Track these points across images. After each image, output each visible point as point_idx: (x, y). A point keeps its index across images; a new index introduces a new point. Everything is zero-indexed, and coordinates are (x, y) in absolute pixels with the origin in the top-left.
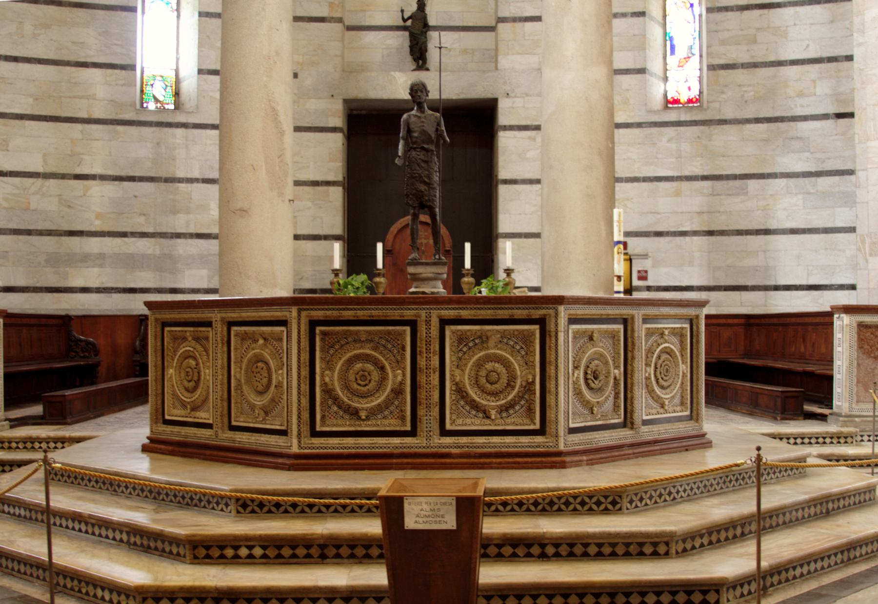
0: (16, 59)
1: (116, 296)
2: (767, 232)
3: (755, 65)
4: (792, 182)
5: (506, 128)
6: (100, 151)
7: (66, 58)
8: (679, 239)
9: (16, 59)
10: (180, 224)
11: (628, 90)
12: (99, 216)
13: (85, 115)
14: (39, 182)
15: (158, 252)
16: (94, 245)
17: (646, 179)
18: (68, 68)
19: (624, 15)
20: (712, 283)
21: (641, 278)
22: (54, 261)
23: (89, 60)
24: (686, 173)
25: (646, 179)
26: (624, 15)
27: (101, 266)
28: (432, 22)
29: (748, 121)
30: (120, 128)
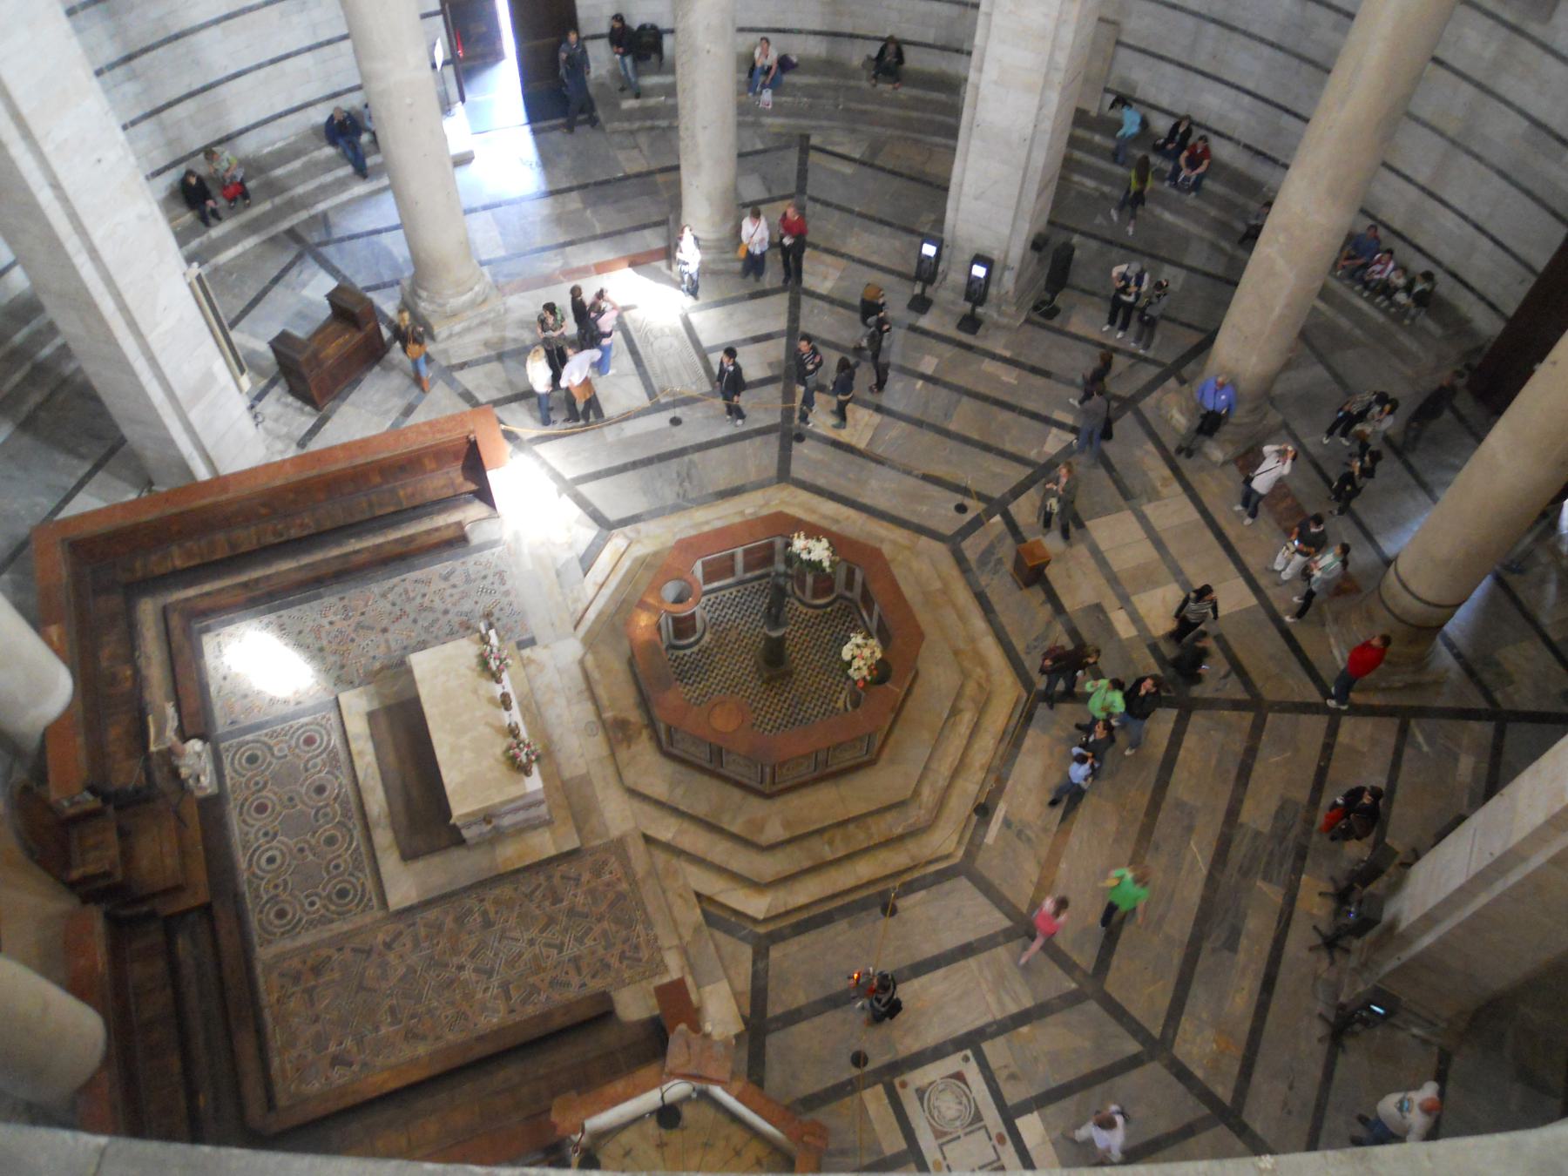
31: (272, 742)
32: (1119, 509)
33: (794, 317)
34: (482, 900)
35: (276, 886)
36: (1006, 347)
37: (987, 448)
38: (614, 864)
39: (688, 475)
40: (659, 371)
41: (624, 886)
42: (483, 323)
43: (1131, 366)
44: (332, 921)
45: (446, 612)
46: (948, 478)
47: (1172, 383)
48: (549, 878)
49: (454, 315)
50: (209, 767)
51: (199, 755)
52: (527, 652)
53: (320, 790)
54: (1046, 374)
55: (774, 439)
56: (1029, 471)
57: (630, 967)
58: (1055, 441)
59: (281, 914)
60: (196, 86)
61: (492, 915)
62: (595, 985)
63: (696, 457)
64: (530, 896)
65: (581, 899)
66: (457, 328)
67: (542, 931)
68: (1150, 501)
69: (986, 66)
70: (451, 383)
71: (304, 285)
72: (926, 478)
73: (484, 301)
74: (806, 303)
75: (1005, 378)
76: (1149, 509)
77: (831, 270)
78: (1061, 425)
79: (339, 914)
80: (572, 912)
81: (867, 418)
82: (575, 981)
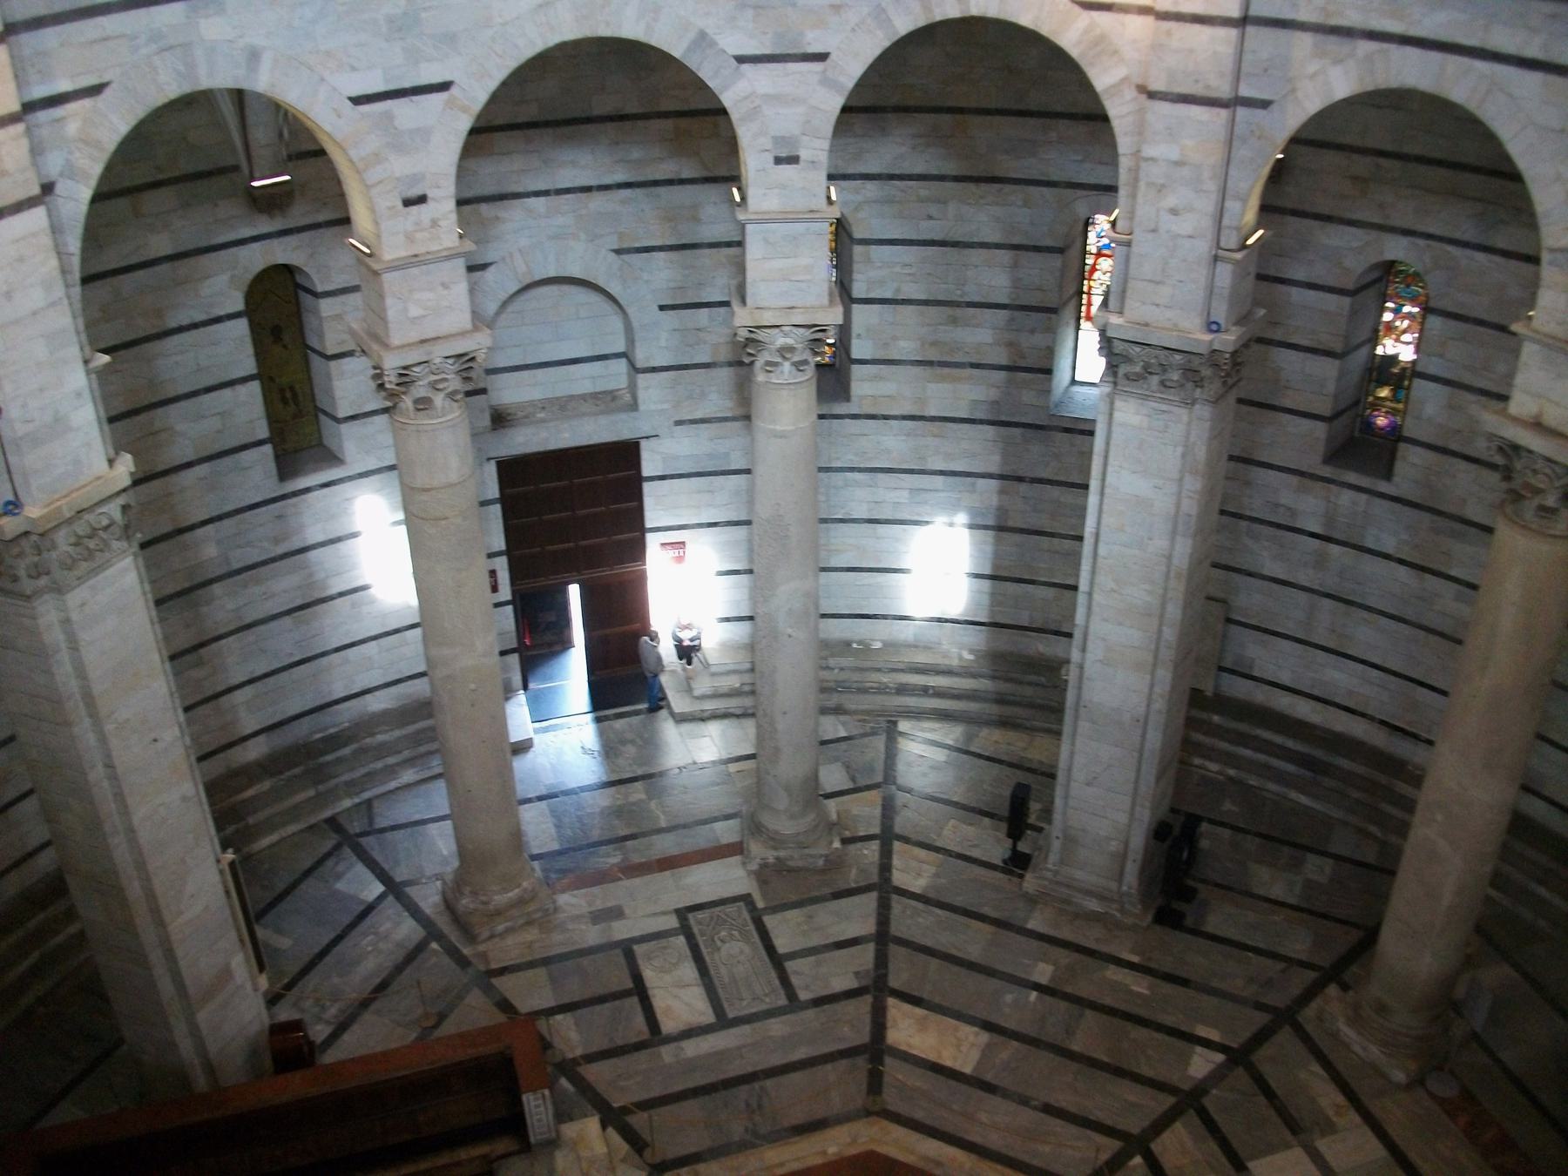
32: (1288, 1146)
33: (883, 920)
36: (1133, 951)
37: (1119, 1072)
39: (760, 1106)
40: (726, 980)
42: (529, 923)
43: (1283, 971)
46: (1073, 1109)
47: (1332, 990)
49: (498, 913)
54: (1185, 982)
55: (862, 1062)
56: (1171, 1100)
58: (1201, 1064)
60: (259, 673)
63: (769, 1083)
66: (500, 928)
68: (1323, 1134)
69: (1090, 646)
70: (488, 989)
71: (339, 877)
72: (1048, 1109)
73: (532, 899)
74: (897, 904)
75: (1135, 988)
76: (1322, 1145)
77: (925, 866)
78: (1207, 1044)
81: (971, 1038)
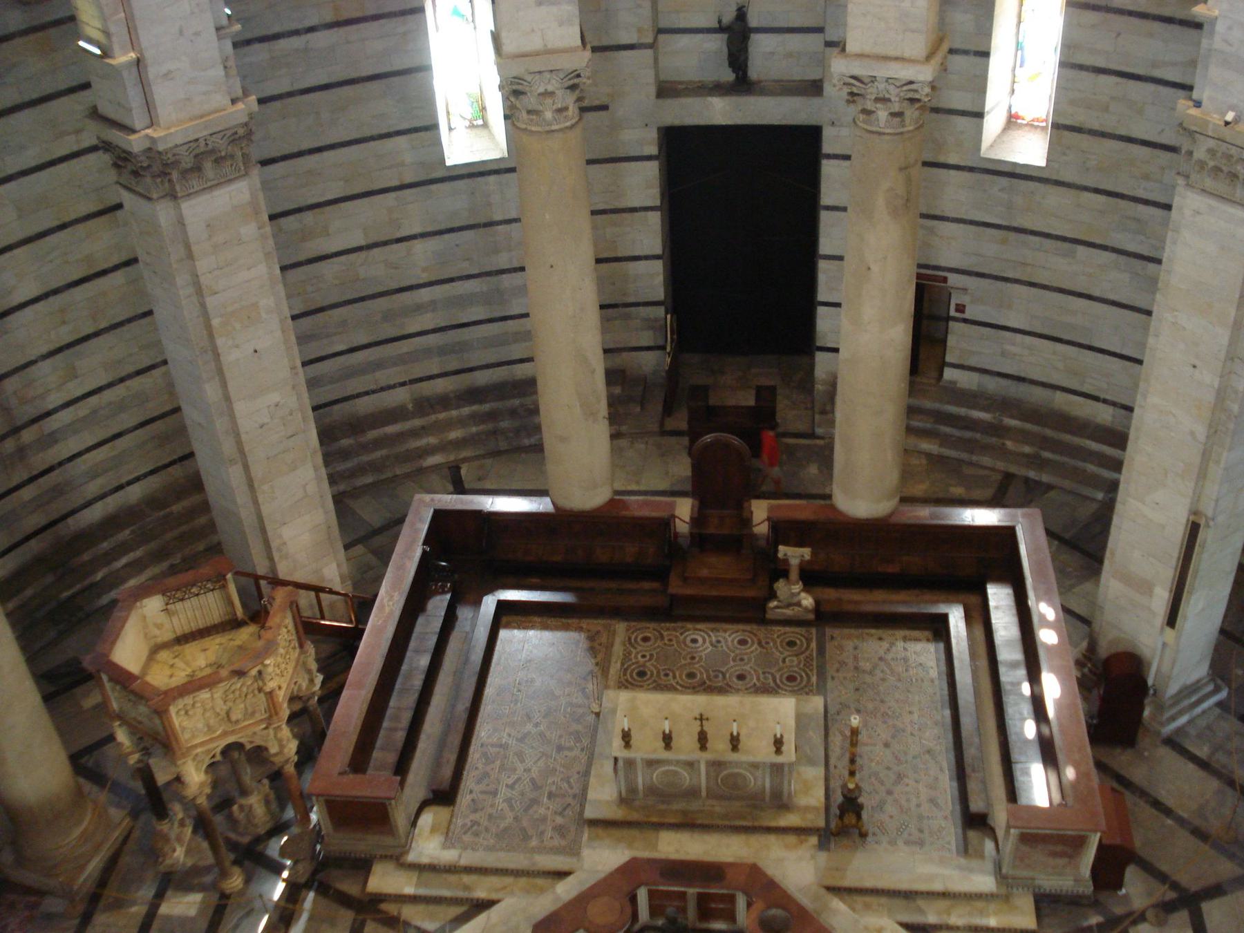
0: (319, 150)
1: (451, 333)
2: (1090, 297)
3: (1103, 135)
4: (1122, 259)
5: (829, 157)
6: (415, 213)
7: (368, 133)
8: (999, 284)
9: (319, 150)
10: (503, 261)
11: (962, 132)
12: (424, 270)
13: (395, 183)
14: (363, 254)
15: (485, 289)
16: (425, 295)
17: (972, 223)
18: (372, 144)
19: (966, 52)
20: (1028, 328)
21: (957, 310)
22: (388, 316)
23: (392, 130)
24: (1015, 224)
25: (972, 223)
26: (966, 52)
27: (433, 311)
28: (753, 22)
29: (1086, 189)
30: (434, 187)
31: (802, 657)
34: (582, 750)
35: (670, 640)
38: (557, 842)
41: (534, 843)
44: (623, 664)
45: (889, 793)
48: (574, 796)
50: (789, 612)
51: (799, 604)
52: (814, 840)
53: (741, 677)
57: (464, 825)
59: (645, 639)
61: (566, 753)
62: (464, 799)
64: (567, 780)
65: (542, 811)
67: (533, 781)
79: (626, 670)
80: (535, 802)
82: (477, 788)
